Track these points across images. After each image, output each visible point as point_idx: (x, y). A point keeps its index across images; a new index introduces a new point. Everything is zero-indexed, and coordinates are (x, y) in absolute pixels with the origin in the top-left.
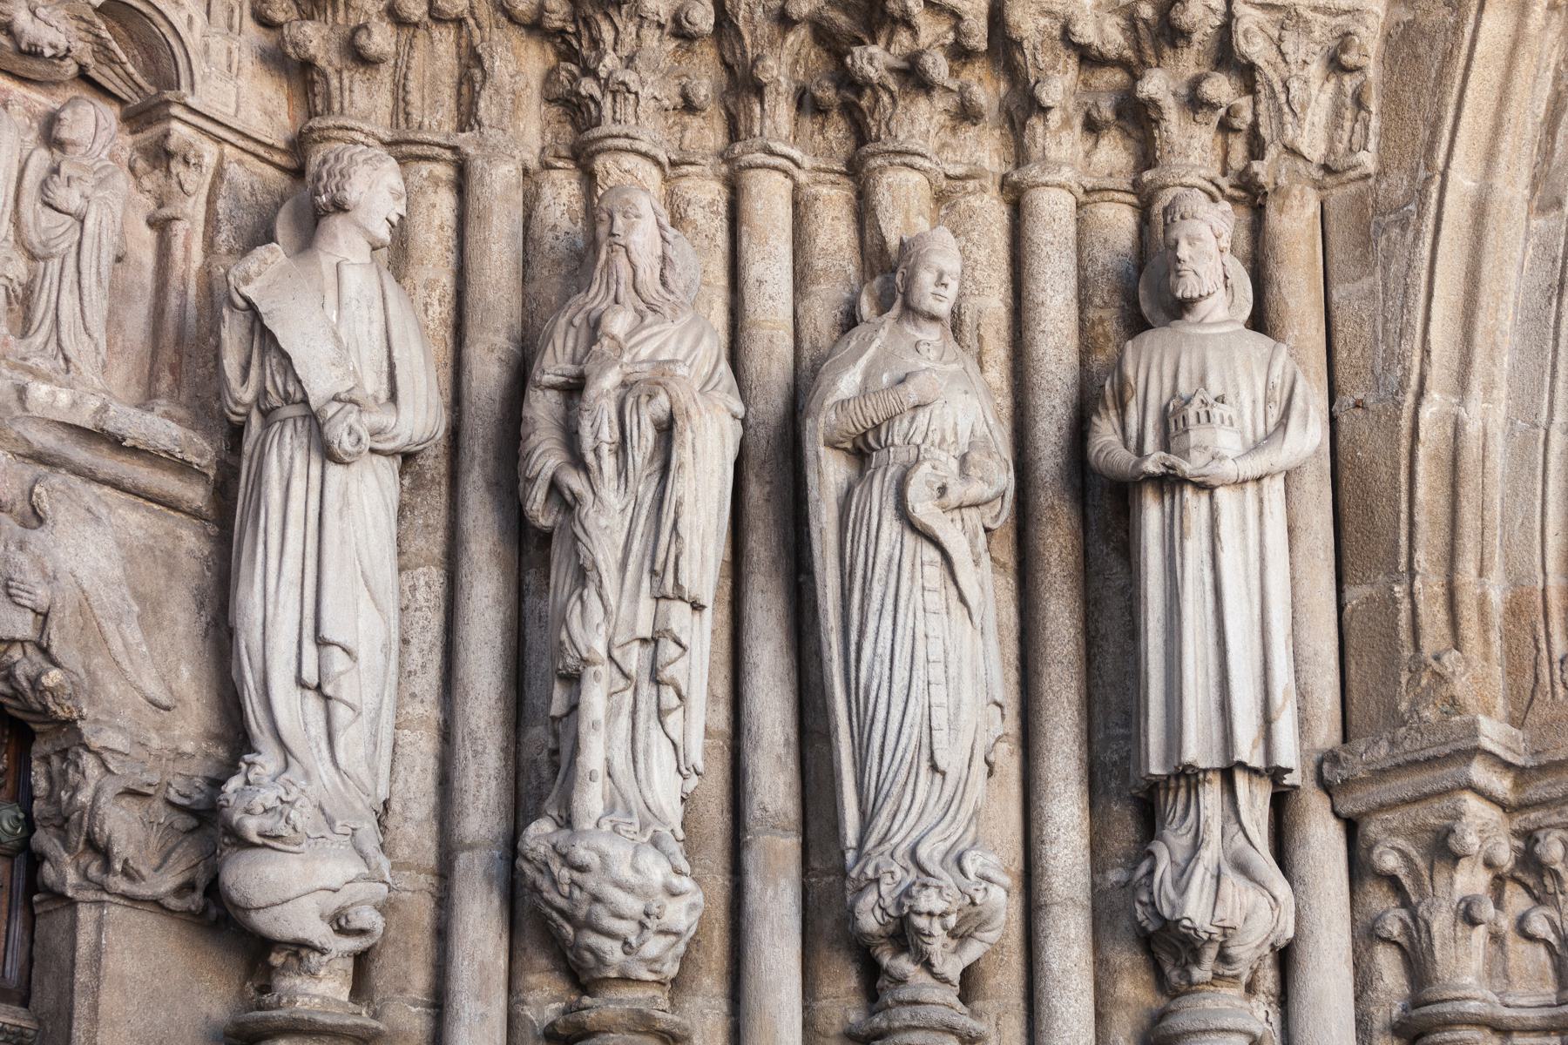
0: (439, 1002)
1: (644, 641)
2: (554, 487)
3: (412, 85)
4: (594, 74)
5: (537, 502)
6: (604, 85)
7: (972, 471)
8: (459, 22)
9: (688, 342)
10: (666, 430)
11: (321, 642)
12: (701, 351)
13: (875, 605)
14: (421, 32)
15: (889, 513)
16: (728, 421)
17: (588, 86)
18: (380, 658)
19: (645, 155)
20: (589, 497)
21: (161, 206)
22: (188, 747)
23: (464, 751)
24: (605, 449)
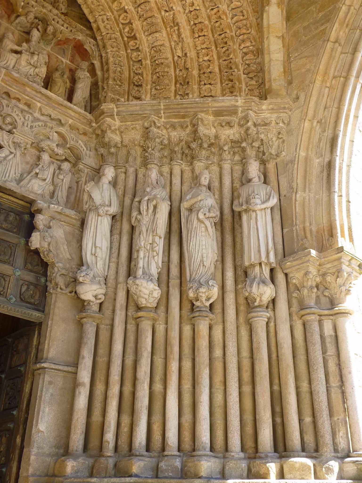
0: (114, 311)
1: (150, 244)
2: (136, 218)
3: (119, 157)
4: (147, 152)
5: (133, 220)
6: (149, 154)
7: (211, 211)
8: (126, 146)
9: (161, 192)
10: (155, 207)
11: (96, 247)
12: (163, 194)
13: (193, 236)
14: (121, 149)
15: (196, 219)
16: (167, 205)
17: (146, 154)
18: (106, 250)
19: (156, 164)
20: (142, 219)
21: (78, 179)
22: (74, 266)
23: (120, 266)
24: (145, 210)
